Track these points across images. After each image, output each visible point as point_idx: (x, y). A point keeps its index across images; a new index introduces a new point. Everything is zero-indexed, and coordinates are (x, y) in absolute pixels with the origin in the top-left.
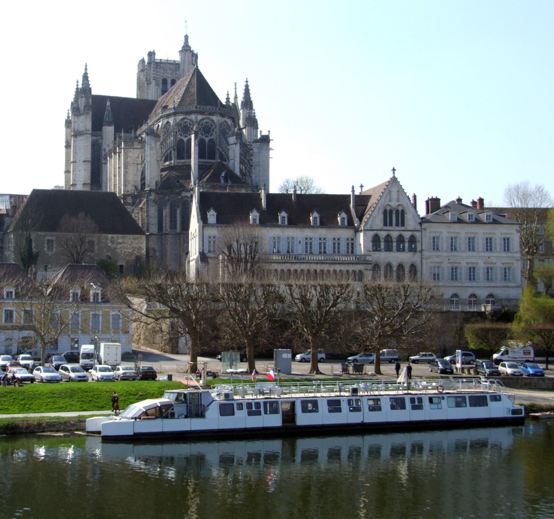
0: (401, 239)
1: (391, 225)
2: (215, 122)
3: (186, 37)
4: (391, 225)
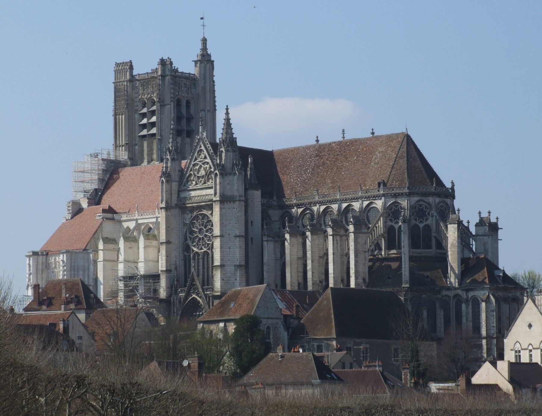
2: (450, 205)
3: (204, 41)
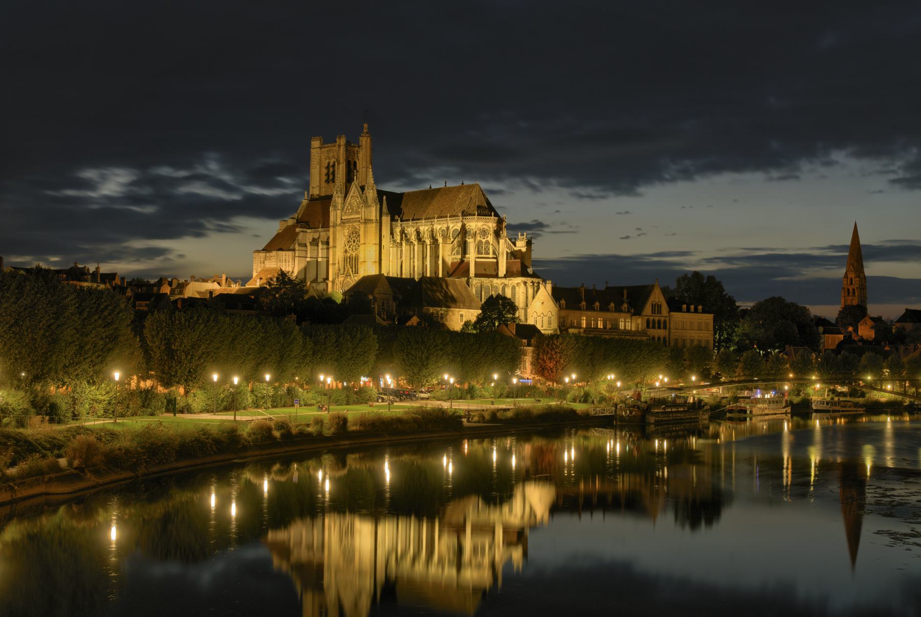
0: (659, 321)
1: (655, 313)
4: (655, 313)
